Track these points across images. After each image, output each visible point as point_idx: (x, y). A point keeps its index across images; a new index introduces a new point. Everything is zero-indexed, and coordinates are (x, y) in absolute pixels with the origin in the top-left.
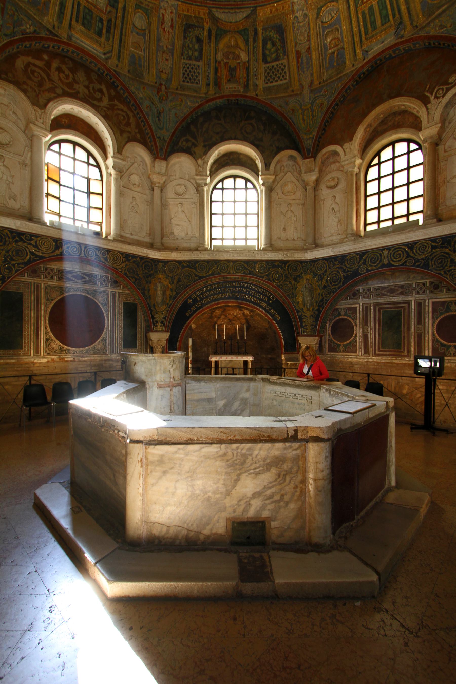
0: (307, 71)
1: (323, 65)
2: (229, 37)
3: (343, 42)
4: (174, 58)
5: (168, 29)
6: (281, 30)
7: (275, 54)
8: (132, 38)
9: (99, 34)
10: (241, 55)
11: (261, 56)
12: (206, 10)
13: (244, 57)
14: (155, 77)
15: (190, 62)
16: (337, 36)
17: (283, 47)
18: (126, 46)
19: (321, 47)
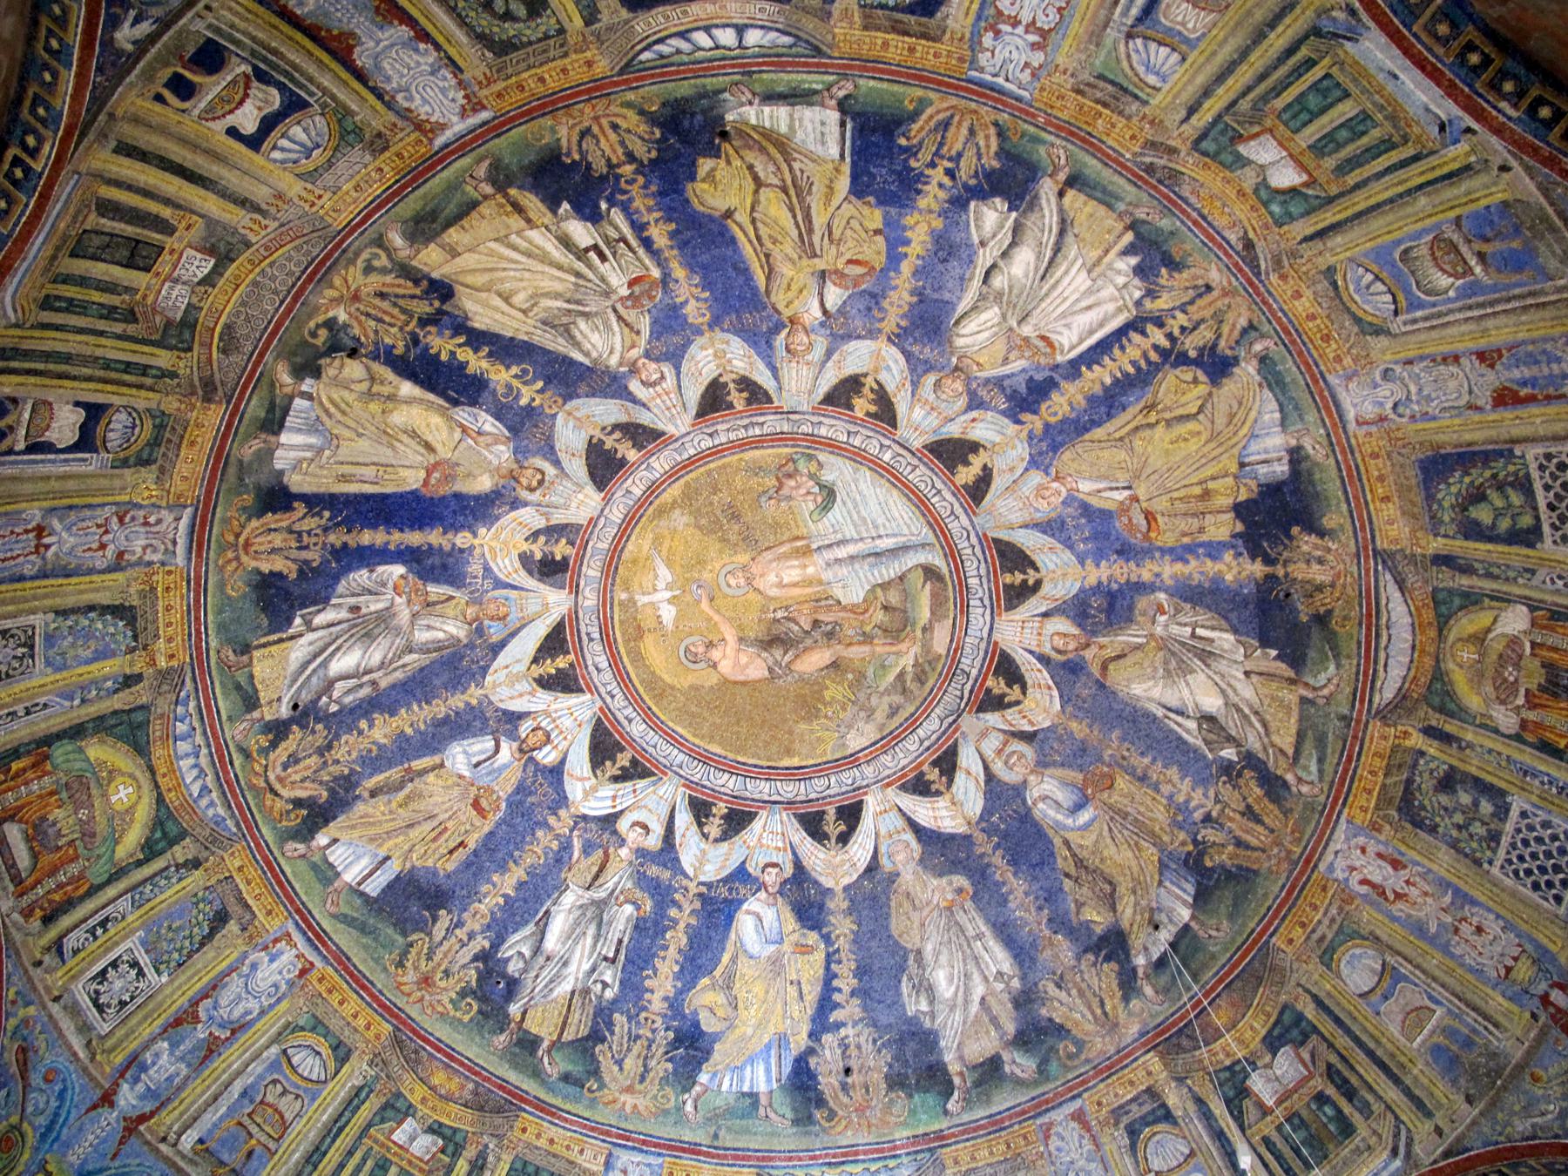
0: (1559, 360)
1: (1532, 294)
2: (1451, 666)
3: (1438, 226)
4: (1483, 899)
5: (1400, 886)
6: (1437, 466)
7: (1509, 490)
8: (1390, 1024)
9: (1347, 1129)
10: (1509, 630)
11: (1515, 549)
12: (1375, 728)
13: (1515, 621)
14: (1515, 1009)
15: (1505, 841)
16: (1424, 251)
17: (1486, 457)
18: (1403, 1059)
19: (1470, 308)
